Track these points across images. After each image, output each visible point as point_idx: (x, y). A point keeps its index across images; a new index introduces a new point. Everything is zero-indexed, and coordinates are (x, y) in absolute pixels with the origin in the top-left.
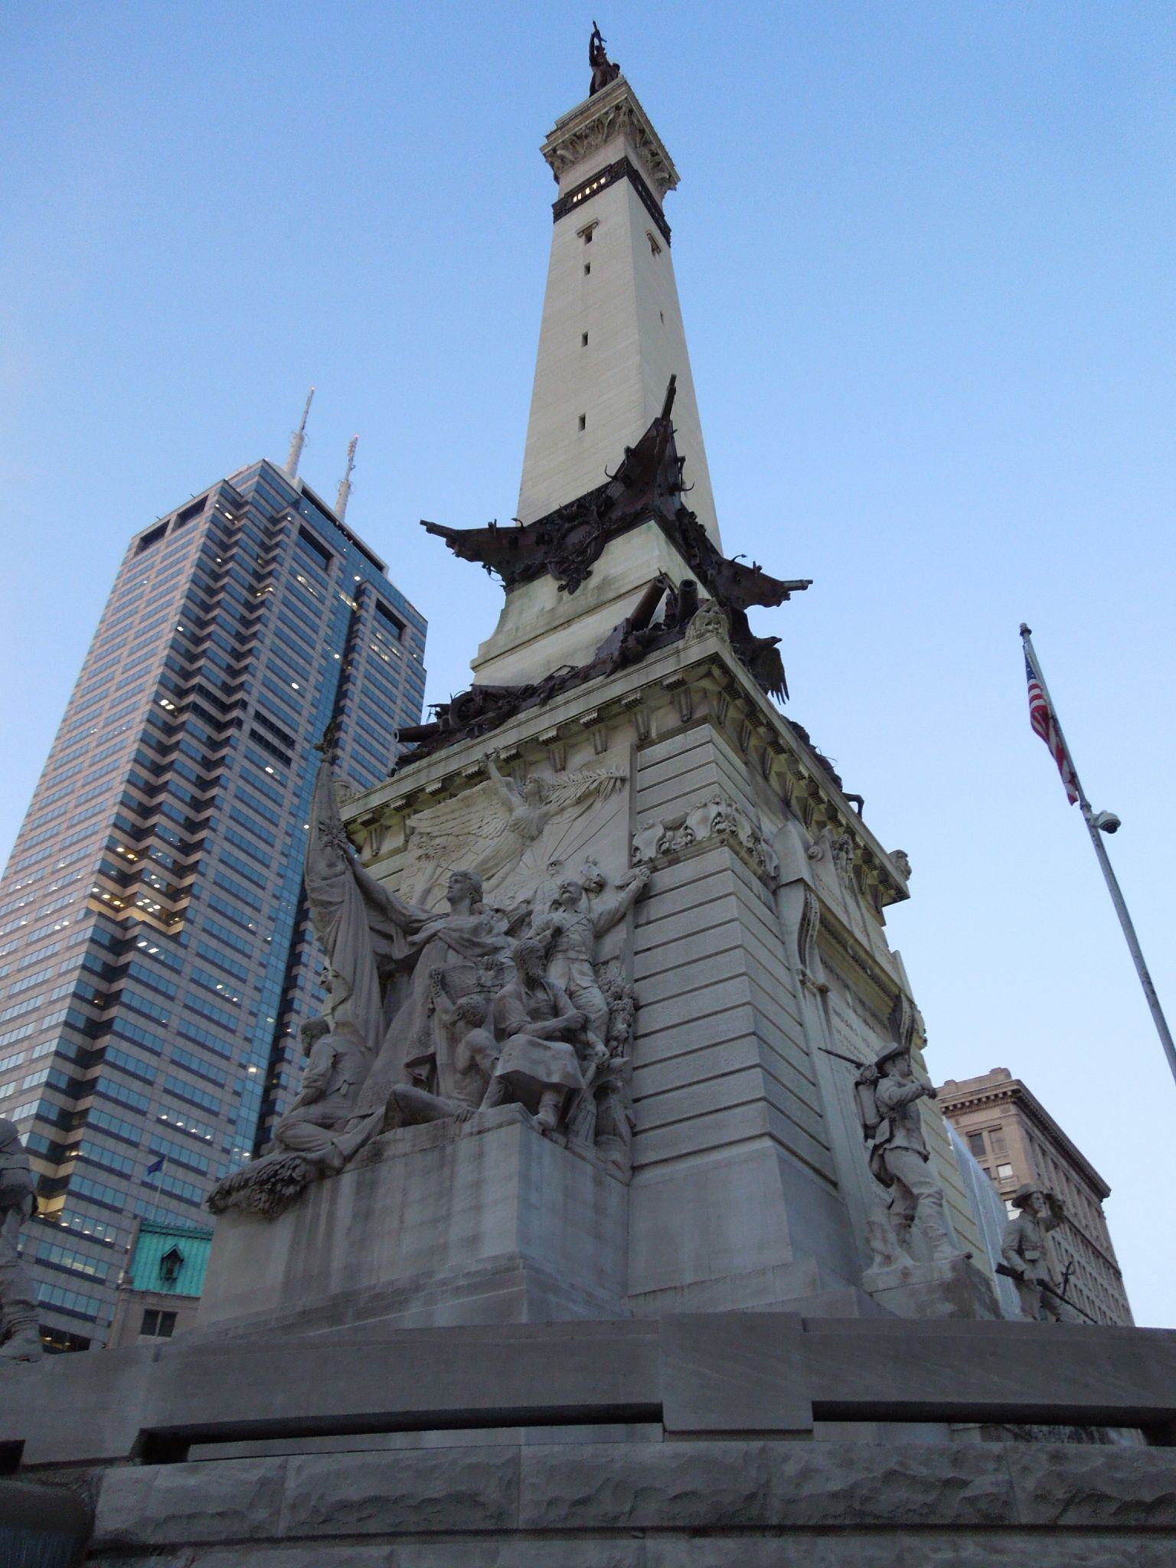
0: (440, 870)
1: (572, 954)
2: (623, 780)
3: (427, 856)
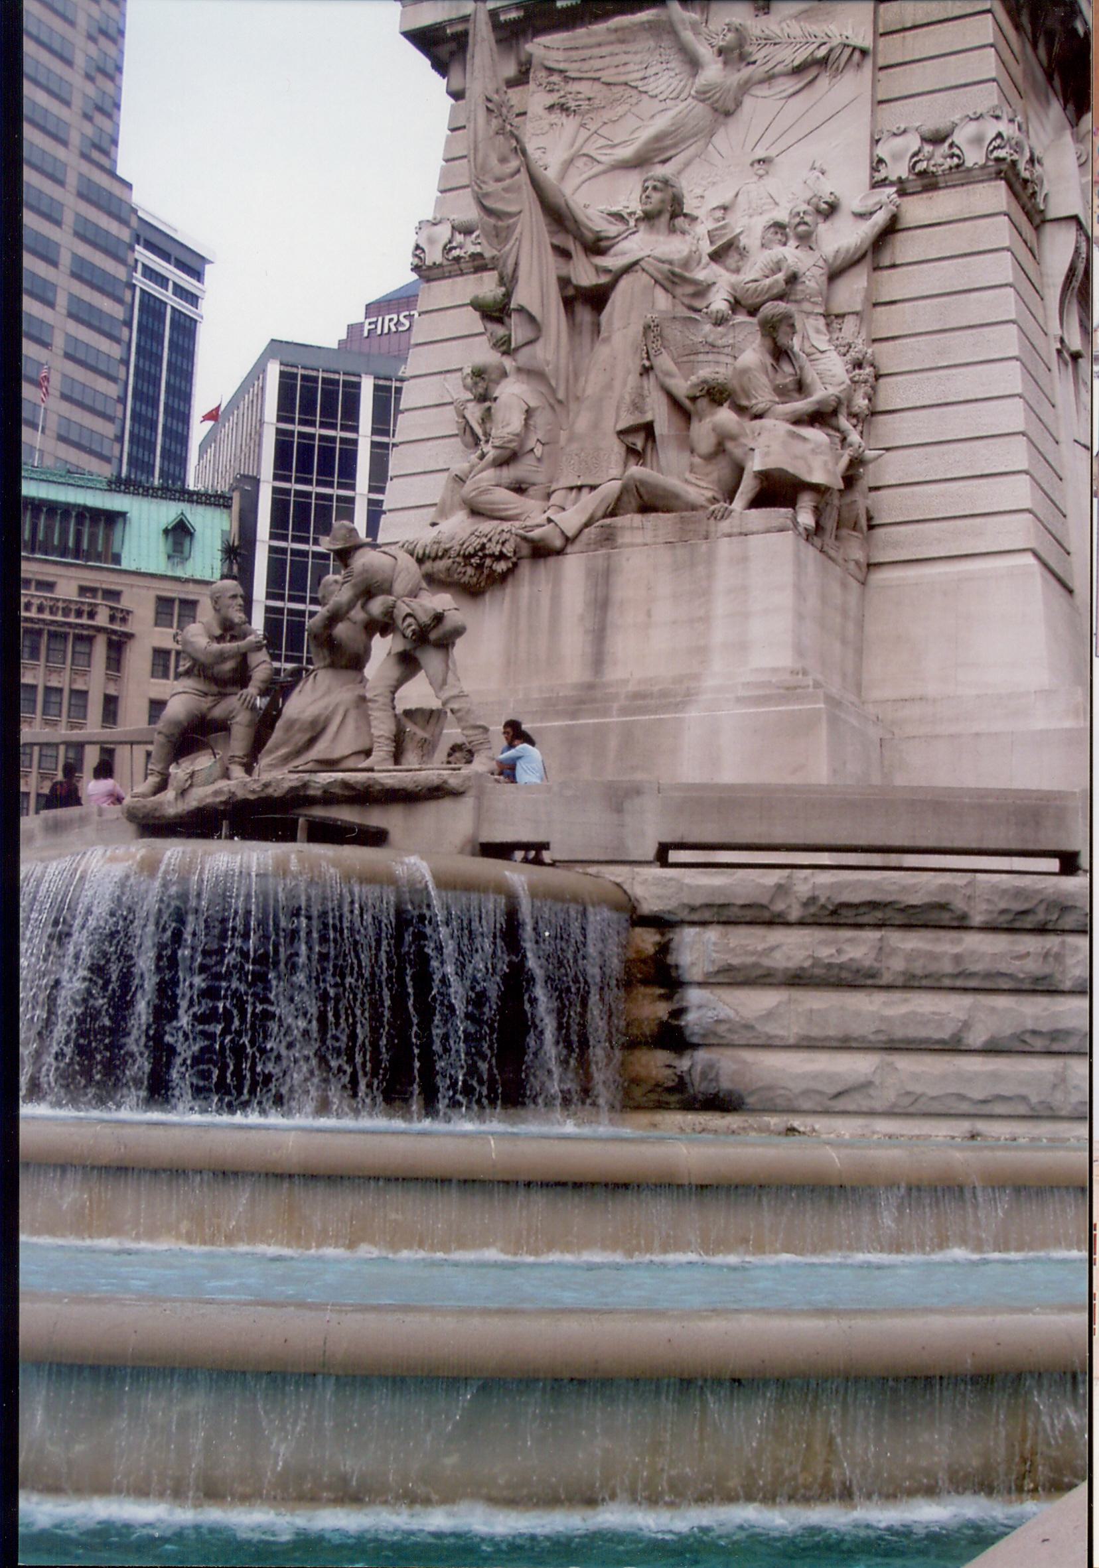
0: (584, 134)
1: (807, 306)
2: (864, 53)
3: (564, 108)
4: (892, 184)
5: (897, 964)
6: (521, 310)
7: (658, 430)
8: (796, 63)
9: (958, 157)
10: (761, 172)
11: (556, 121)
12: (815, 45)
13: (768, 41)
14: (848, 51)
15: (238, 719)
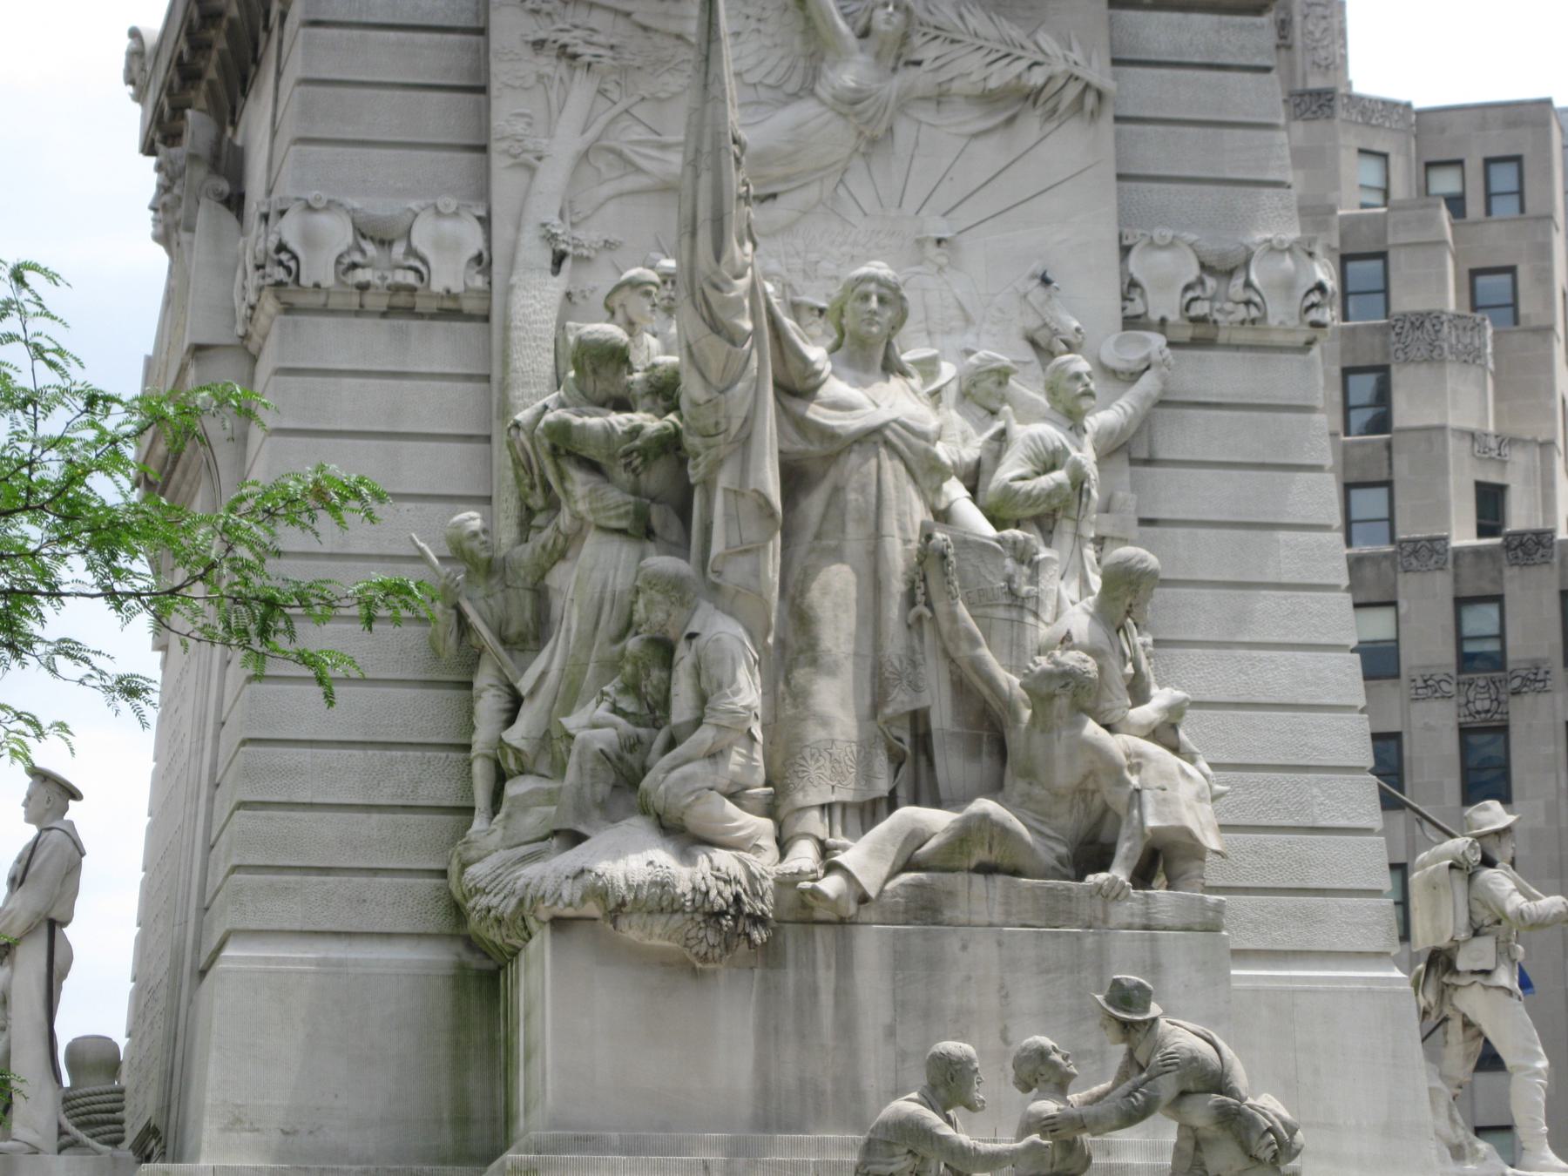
3: (567, 55)
7: (942, 719)
8: (993, 84)
10: (943, 260)
11: (549, 70)
12: (1023, 64)
14: (1073, 91)
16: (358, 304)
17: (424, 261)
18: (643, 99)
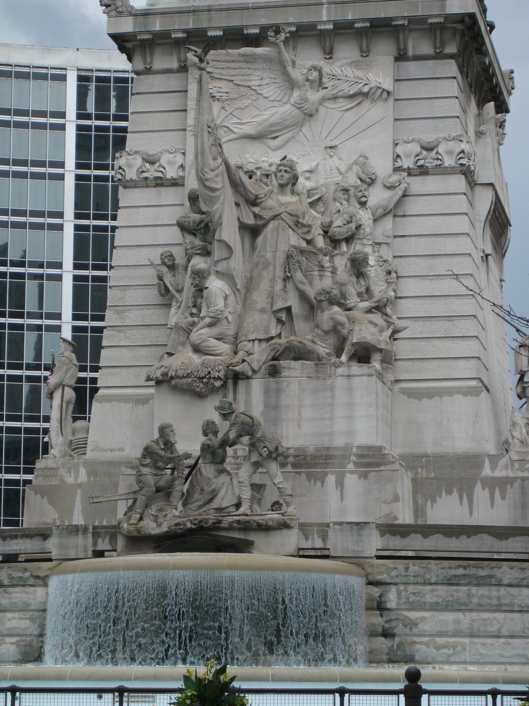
1: (365, 241)
2: (389, 93)
4: (404, 170)
5: (475, 600)
6: (220, 241)
7: (294, 311)
8: (351, 93)
9: (441, 160)
12: (362, 84)
13: (333, 77)
14: (379, 92)
15: (177, 489)
16: (145, 183)
17: (164, 168)
18: (237, 109)
